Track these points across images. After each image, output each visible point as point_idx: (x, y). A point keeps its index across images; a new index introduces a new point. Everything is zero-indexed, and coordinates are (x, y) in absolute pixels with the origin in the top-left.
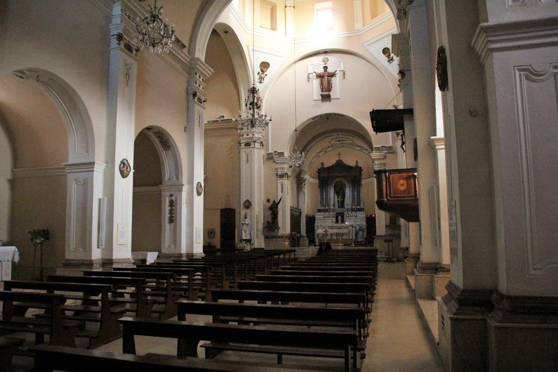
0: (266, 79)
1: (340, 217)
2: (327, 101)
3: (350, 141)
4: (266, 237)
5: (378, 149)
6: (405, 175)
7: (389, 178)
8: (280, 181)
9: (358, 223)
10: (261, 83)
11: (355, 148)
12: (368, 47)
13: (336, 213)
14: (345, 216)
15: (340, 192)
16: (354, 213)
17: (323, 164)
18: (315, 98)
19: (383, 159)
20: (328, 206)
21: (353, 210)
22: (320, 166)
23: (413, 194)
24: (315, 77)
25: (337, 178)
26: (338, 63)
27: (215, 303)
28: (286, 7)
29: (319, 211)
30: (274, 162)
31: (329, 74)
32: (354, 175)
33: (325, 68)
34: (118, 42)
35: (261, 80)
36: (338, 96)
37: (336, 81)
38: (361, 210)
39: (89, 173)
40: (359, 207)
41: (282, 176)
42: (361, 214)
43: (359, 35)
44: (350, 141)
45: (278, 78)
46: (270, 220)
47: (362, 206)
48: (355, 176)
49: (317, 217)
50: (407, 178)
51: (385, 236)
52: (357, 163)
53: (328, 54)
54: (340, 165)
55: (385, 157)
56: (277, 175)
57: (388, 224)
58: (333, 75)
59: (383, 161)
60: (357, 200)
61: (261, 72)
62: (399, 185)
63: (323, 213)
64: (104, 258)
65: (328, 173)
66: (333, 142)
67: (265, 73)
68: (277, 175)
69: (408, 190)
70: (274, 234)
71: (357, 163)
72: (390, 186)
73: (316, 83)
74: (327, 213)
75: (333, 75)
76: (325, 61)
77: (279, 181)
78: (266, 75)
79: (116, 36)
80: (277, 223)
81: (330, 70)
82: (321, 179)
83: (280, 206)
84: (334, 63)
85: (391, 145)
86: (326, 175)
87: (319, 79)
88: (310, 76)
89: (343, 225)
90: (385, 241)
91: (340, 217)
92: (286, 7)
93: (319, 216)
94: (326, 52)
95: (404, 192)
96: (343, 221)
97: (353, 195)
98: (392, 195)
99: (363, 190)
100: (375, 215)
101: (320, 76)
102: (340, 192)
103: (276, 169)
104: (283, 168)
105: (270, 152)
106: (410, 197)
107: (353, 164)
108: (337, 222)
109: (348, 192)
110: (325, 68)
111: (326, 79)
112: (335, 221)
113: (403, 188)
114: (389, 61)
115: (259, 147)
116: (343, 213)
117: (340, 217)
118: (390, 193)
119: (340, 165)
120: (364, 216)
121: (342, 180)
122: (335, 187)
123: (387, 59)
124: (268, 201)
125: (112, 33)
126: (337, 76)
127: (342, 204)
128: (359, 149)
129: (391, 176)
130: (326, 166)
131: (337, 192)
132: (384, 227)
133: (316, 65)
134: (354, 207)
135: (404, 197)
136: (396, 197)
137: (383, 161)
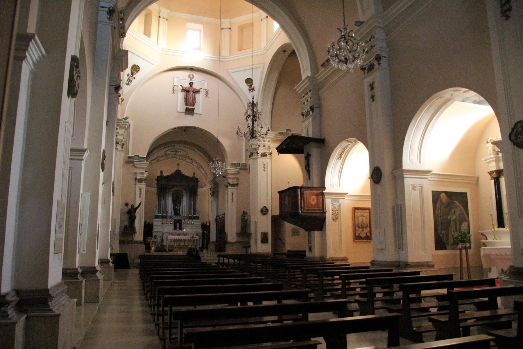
0: (134, 82)
1: (178, 224)
2: (190, 114)
3: (185, 153)
4: (121, 242)
5: (233, 165)
6: (315, 192)
7: (303, 194)
8: (139, 185)
9: (195, 230)
10: (128, 84)
11: (187, 160)
12: (232, 74)
13: (175, 220)
15: (177, 201)
16: (190, 220)
17: (161, 172)
18: (179, 110)
19: (236, 174)
20: (167, 212)
21: (190, 218)
22: (159, 174)
23: (321, 208)
24: (180, 91)
25: (175, 187)
26: (202, 82)
27: (261, 305)
28: (160, 17)
29: (157, 217)
30: (134, 166)
31: (194, 90)
32: (191, 186)
33: (191, 84)
34: (108, 16)
35: (129, 81)
36: (201, 112)
37: (200, 98)
38: (197, 218)
39: (78, 161)
41: (140, 181)
42: (196, 222)
43: (225, 62)
44: (185, 153)
45: (145, 83)
46: (126, 223)
47: (197, 215)
48: (193, 186)
49: (154, 223)
50: (317, 195)
51: (236, 242)
52: (194, 173)
53: (193, 72)
54: (178, 174)
55: (239, 173)
56: (136, 179)
57: (239, 232)
58: (198, 91)
59: (237, 176)
60: (193, 208)
61: (130, 74)
62: (311, 200)
63: (161, 220)
64: (82, 266)
66: (168, 152)
67: (134, 76)
68: (136, 179)
69: (317, 205)
70: (130, 239)
71: (194, 173)
72: (304, 201)
73: (181, 96)
74: (165, 220)
75: (198, 91)
76: (191, 77)
77: (137, 186)
78: (134, 78)
79: (107, 9)
80: (134, 227)
81: (195, 86)
83: (138, 210)
84: (199, 81)
85: (244, 162)
87: (184, 93)
88: (176, 88)
89: (180, 231)
90: (244, 247)
91: (178, 224)
92: (160, 17)
93: (156, 223)
94: (192, 69)
95: (314, 206)
96: (181, 228)
97: (190, 204)
98: (306, 208)
99: (199, 199)
100: (210, 224)
101: (186, 91)
102: (177, 201)
103: (136, 173)
104: (143, 173)
105: (130, 155)
106: (319, 210)
107: (191, 175)
108: (175, 228)
109: (185, 200)
110: (191, 84)
111: (190, 94)
112: (173, 227)
113: (314, 203)
114: (250, 90)
115: (121, 149)
116: (181, 221)
117: (178, 225)
118: (304, 206)
119: (178, 174)
120: (199, 224)
121: (178, 188)
122: (173, 195)
123: (248, 87)
124: (127, 205)
125: (102, 4)
126: (201, 93)
128: (190, 161)
129: (305, 192)
130: (165, 174)
131: (174, 201)
132: (235, 235)
133: (182, 79)
135: (314, 210)
136: (309, 210)
137: (237, 176)
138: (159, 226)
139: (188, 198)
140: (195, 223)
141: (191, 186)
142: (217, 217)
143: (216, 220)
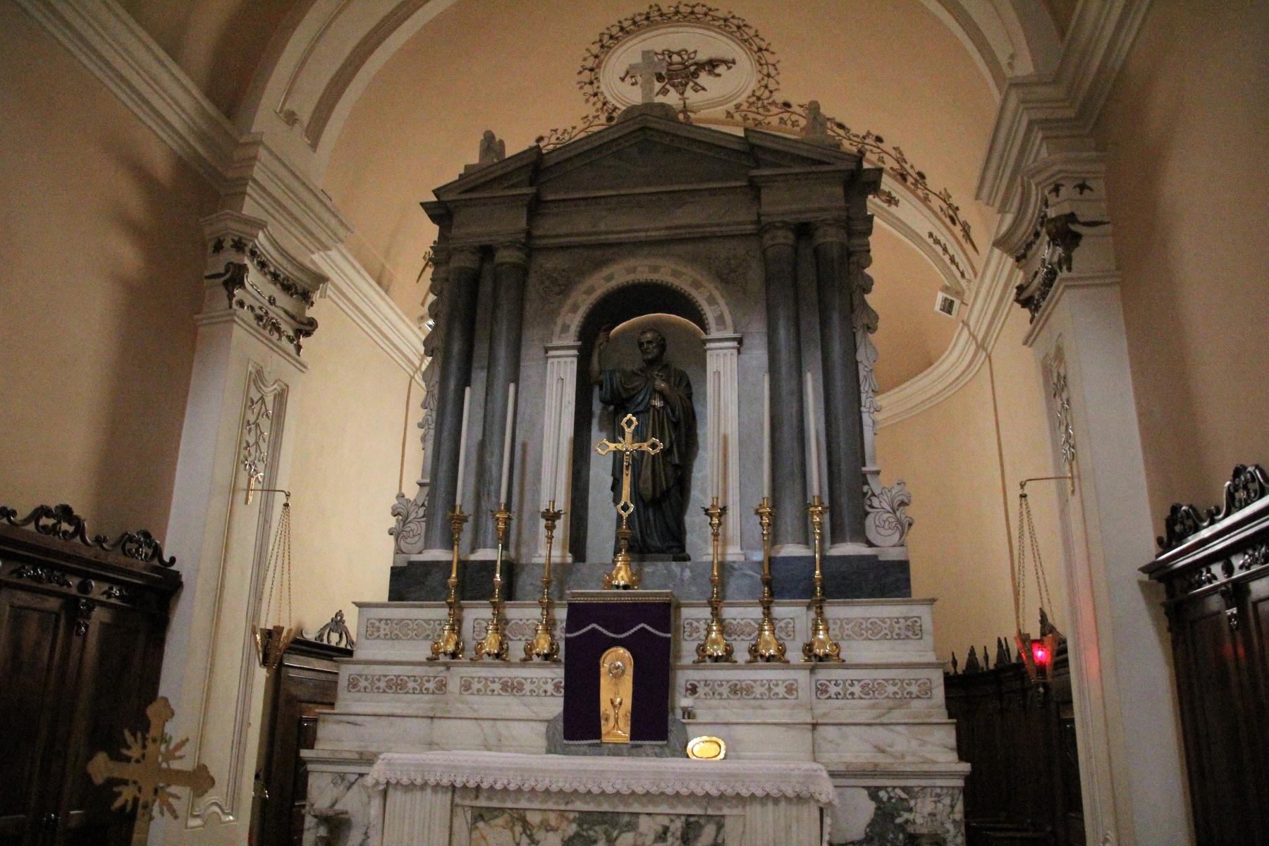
1: (617, 660)
9: (854, 748)
13: (579, 614)
14: (688, 650)
16: (792, 613)
21: (779, 582)
38: (888, 580)
40: (849, 549)
42: (873, 631)
48: (803, 231)
54: (647, 147)
65: (535, 207)
82: (459, 261)
86: (502, 225)
91: (617, 660)
96: (654, 721)
100: (1061, 650)
102: (641, 387)
108: (580, 722)
109: (731, 388)
112: (555, 706)
127: (659, 518)
131: (601, 398)
134: (792, 550)
138: (397, 685)
139: (758, 355)
140: (856, 651)
141: (801, 233)
142: (1177, 525)
143: (1173, 589)
